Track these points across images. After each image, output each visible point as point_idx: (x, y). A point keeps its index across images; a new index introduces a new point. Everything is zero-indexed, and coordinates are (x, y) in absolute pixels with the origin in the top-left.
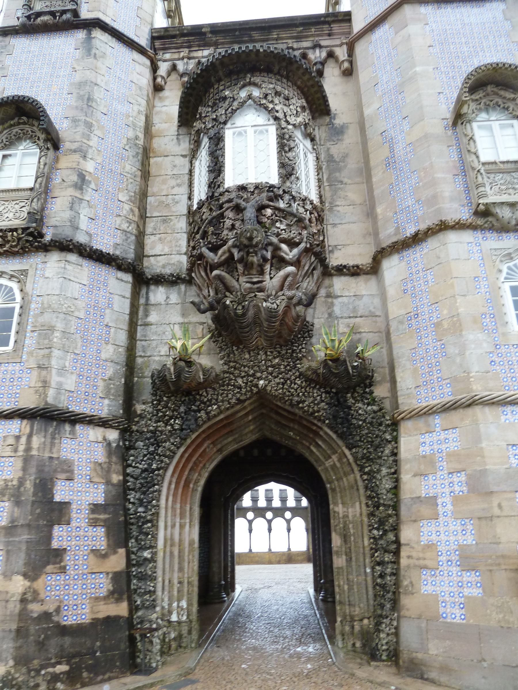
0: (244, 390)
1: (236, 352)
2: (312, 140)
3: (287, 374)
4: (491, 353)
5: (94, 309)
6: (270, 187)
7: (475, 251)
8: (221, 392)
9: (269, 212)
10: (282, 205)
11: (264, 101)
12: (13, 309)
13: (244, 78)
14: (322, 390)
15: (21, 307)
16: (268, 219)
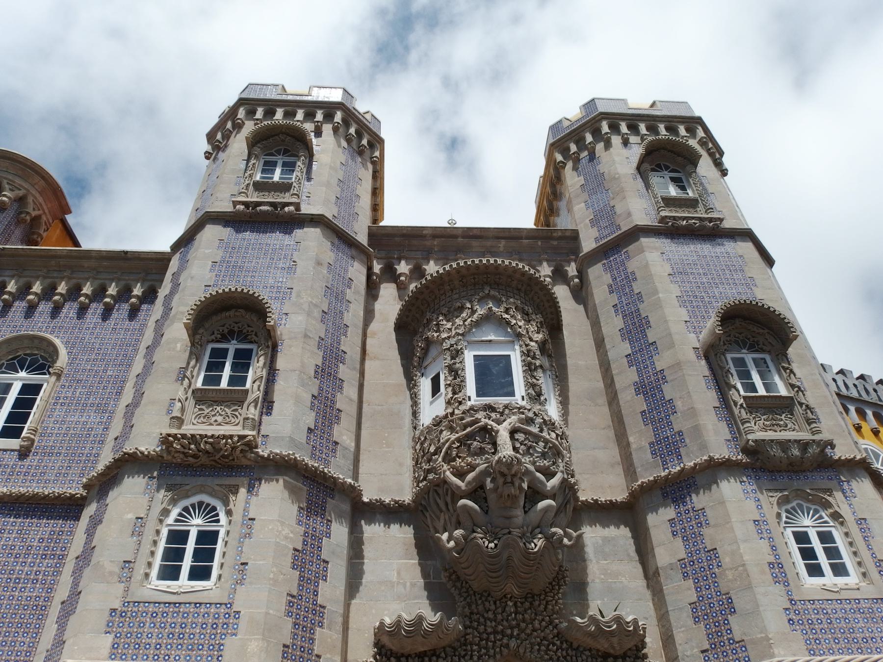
0: (492, 652)
1: (479, 602)
2: (549, 356)
3: (542, 631)
4: (786, 609)
5: (312, 539)
6: (519, 408)
7: (749, 491)
8: (463, 653)
9: (520, 436)
10: (535, 430)
11: (506, 316)
12: (217, 532)
13: (482, 289)
14: (587, 653)
15: (228, 532)
16: (521, 444)
